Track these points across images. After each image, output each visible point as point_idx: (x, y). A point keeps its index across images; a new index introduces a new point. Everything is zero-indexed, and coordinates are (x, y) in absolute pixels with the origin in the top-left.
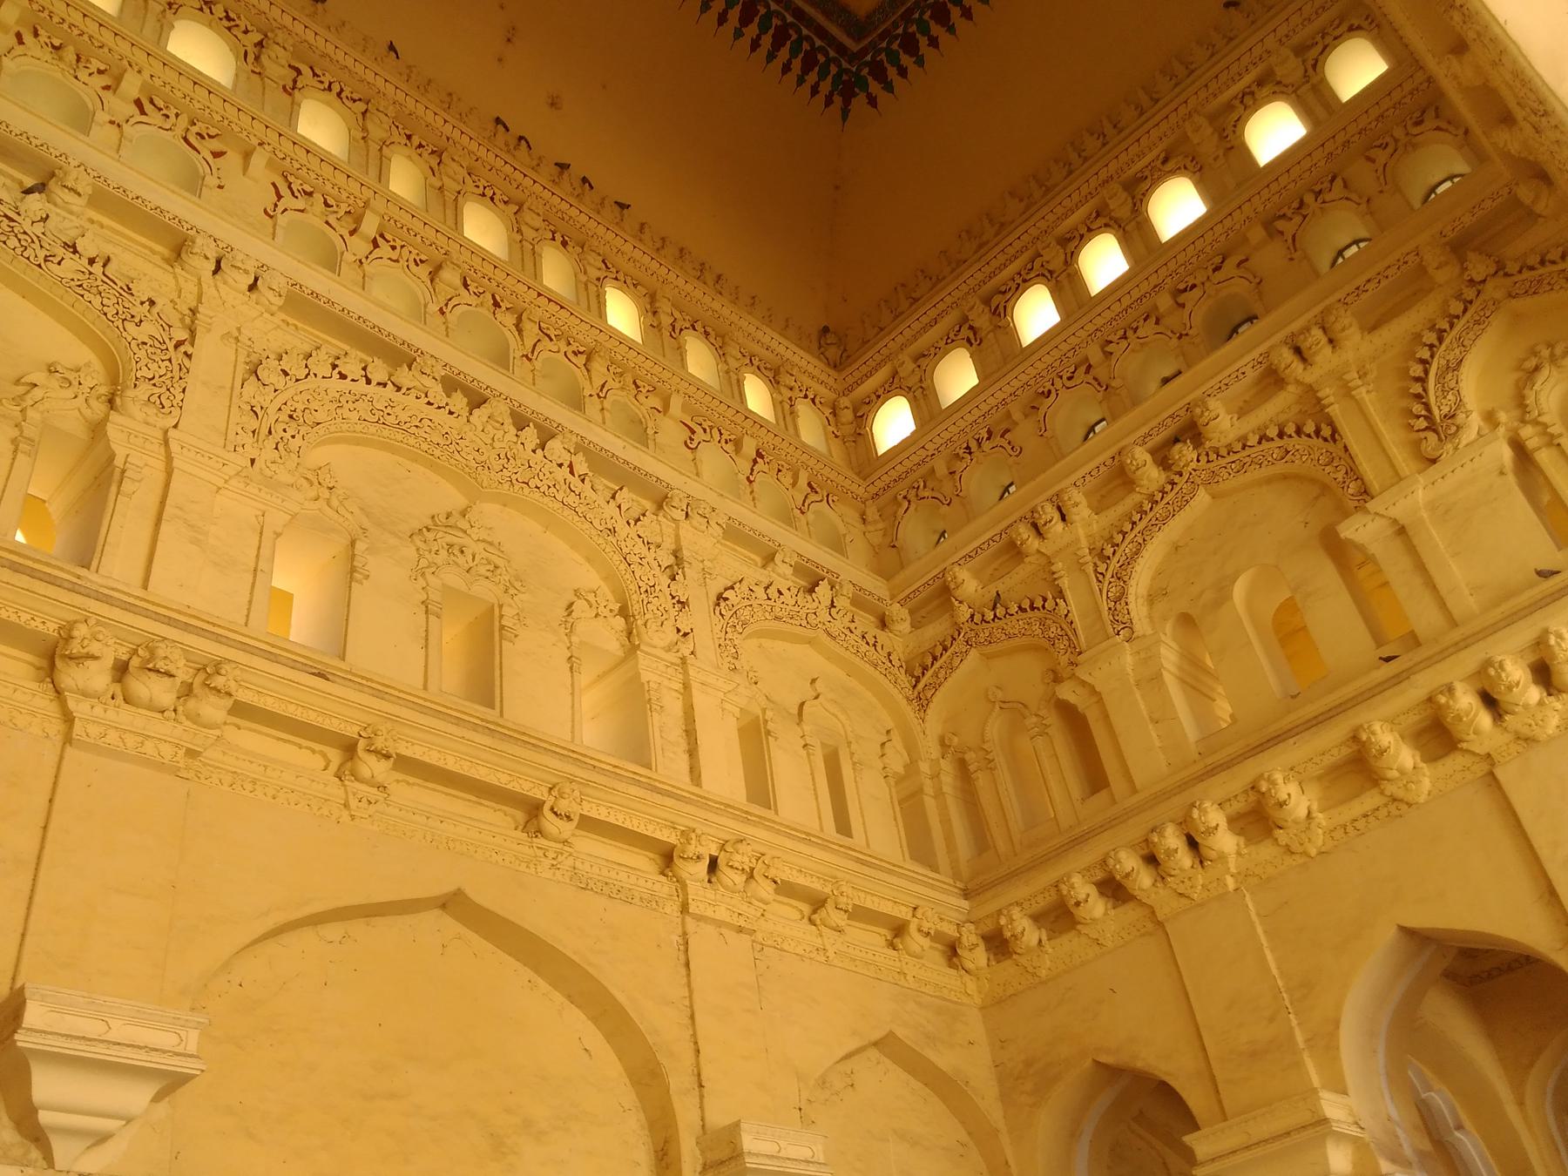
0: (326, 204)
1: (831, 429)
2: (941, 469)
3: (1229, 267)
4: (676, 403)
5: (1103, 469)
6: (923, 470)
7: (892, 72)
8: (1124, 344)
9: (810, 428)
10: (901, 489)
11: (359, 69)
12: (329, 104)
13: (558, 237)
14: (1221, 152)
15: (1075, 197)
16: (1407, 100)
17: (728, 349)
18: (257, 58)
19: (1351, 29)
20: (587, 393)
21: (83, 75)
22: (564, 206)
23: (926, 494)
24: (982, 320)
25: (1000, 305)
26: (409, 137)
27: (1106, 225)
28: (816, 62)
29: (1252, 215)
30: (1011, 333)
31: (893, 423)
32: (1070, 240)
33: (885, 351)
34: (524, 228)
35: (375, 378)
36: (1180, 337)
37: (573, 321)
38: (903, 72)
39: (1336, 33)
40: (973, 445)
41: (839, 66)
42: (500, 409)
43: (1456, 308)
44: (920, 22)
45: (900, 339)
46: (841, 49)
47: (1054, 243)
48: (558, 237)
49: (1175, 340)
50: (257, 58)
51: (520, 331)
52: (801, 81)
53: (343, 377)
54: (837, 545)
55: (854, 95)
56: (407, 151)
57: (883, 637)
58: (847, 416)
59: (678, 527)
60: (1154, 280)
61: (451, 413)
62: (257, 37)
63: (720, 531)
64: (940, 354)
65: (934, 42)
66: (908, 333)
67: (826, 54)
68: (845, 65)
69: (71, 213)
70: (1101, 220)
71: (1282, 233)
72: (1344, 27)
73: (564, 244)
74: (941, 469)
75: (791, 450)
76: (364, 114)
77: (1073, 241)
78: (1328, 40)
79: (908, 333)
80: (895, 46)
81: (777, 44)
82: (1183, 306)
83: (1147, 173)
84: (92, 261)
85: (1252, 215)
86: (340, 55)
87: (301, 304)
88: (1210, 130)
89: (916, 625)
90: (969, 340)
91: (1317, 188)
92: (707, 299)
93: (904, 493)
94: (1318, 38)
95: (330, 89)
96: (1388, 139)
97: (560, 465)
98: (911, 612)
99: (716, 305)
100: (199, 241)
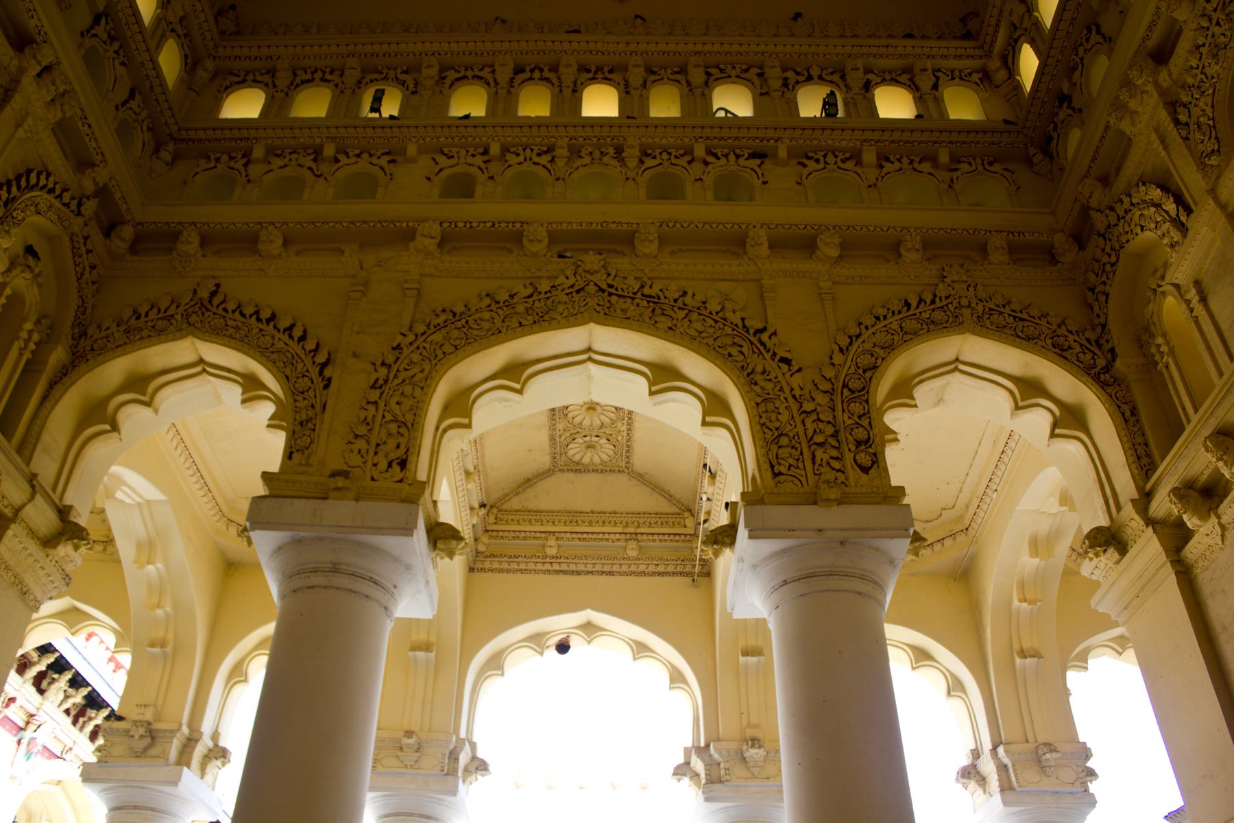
19: (186, 57)
43: (66, 200)
91: (121, 53)
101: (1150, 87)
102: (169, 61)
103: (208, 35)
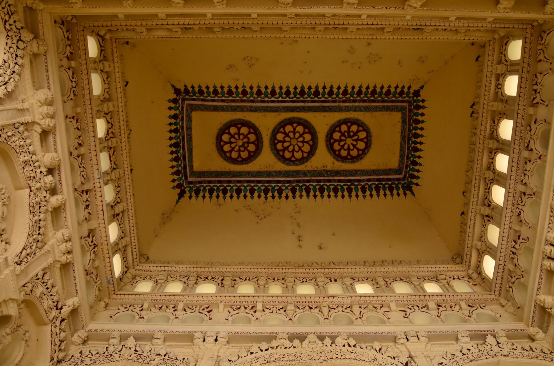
0: (245, 308)
1: (471, 283)
2: (510, 267)
3: (533, 126)
4: (393, 306)
5: (552, 218)
6: (506, 272)
7: (416, 174)
8: (527, 177)
9: (462, 287)
10: (505, 285)
11: (252, 270)
12: (247, 284)
13: (333, 280)
14: (505, 105)
15: (480, 154)
16: (532, 38)
17: (412, 280)
18: (222, 283)
19: (506, 44)
20: (354, 319)
21: (168, 310)
22: (330, 270)
23: (514, 279)
24: (487, 211)
25: (488, 202)
26: (274, 279)
27: (495, 153)
28: (393, 187)
29: (524, 107)
30: (497, 207)
31: (489, 265)
32: (490, 167)
33: (469, 246)
34: (318, 283)
35: (264, 349)
36: (540, 158)
37: (340, 299)
38: (418, 171)
39: (504, 49)
40: (514, 250)
41: (401, 184)
42: (312, 338)
44: (412, 156)
45: (470, 238)
46: (398, 179)
47: (485, 171)
48: (333, 280)
49: (539, 161)
50: (222, 283)
51: (322, 312)
52: (392, 195)
53: (252, 353)
54: (495, 320)
55: (412, 187)
56: (274, 283)
57: (533, 345)
58: (475, 275)
59: (406, 346)
60: (516, 151)
61: (294, 347)
62: (221, 278)
63: (426, 339)
64: (485, 232)
65: (419, 157)
66: (471, 234)
67: (395, 184)
68: (403, 182)
69: (159, 345)
70: (493, 153)
71: (538, 103)
72: (504, 46)
73: (336, 281)
74: (510, 267)
75: (451, 297)
76: (258, 280)
77: (491, 166)
78: (503, 53)
79: (471, 234)
80: (411, 167)
81: (378, 190)
82: (531, 150)
83: (492, 130)
84: (165, 356)
85: (524, 107)
86: (246, 270)
87: (232, 339)
88: (496, 103)
89: (545, 332)
90: (489, 221)
91: (535, 83)
92: (395, 269)
93: (508, 286)
94: (501, 55)
95: (246, 280)
96: (539, 52)
97: (344, 346)
98: (541, 327)
99: (400, 269)
100: (195, 334)
101: (42, 122)
102: (515, 50)
103: (491, 48)
